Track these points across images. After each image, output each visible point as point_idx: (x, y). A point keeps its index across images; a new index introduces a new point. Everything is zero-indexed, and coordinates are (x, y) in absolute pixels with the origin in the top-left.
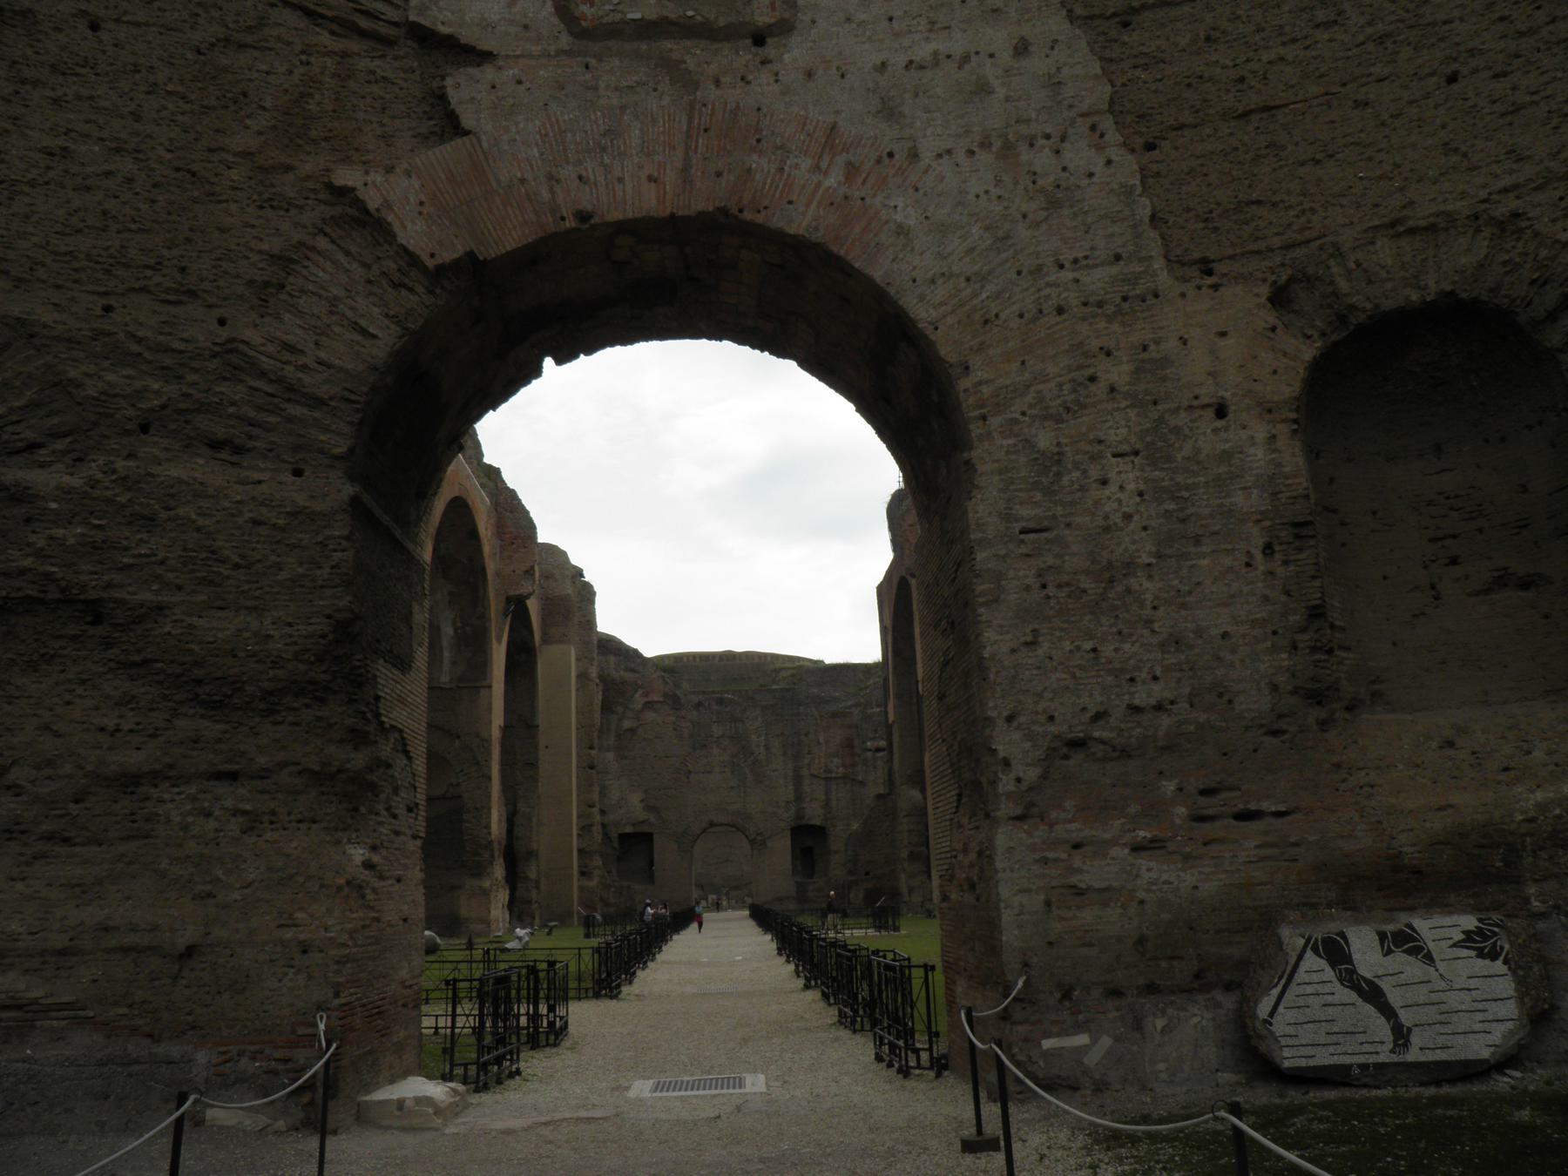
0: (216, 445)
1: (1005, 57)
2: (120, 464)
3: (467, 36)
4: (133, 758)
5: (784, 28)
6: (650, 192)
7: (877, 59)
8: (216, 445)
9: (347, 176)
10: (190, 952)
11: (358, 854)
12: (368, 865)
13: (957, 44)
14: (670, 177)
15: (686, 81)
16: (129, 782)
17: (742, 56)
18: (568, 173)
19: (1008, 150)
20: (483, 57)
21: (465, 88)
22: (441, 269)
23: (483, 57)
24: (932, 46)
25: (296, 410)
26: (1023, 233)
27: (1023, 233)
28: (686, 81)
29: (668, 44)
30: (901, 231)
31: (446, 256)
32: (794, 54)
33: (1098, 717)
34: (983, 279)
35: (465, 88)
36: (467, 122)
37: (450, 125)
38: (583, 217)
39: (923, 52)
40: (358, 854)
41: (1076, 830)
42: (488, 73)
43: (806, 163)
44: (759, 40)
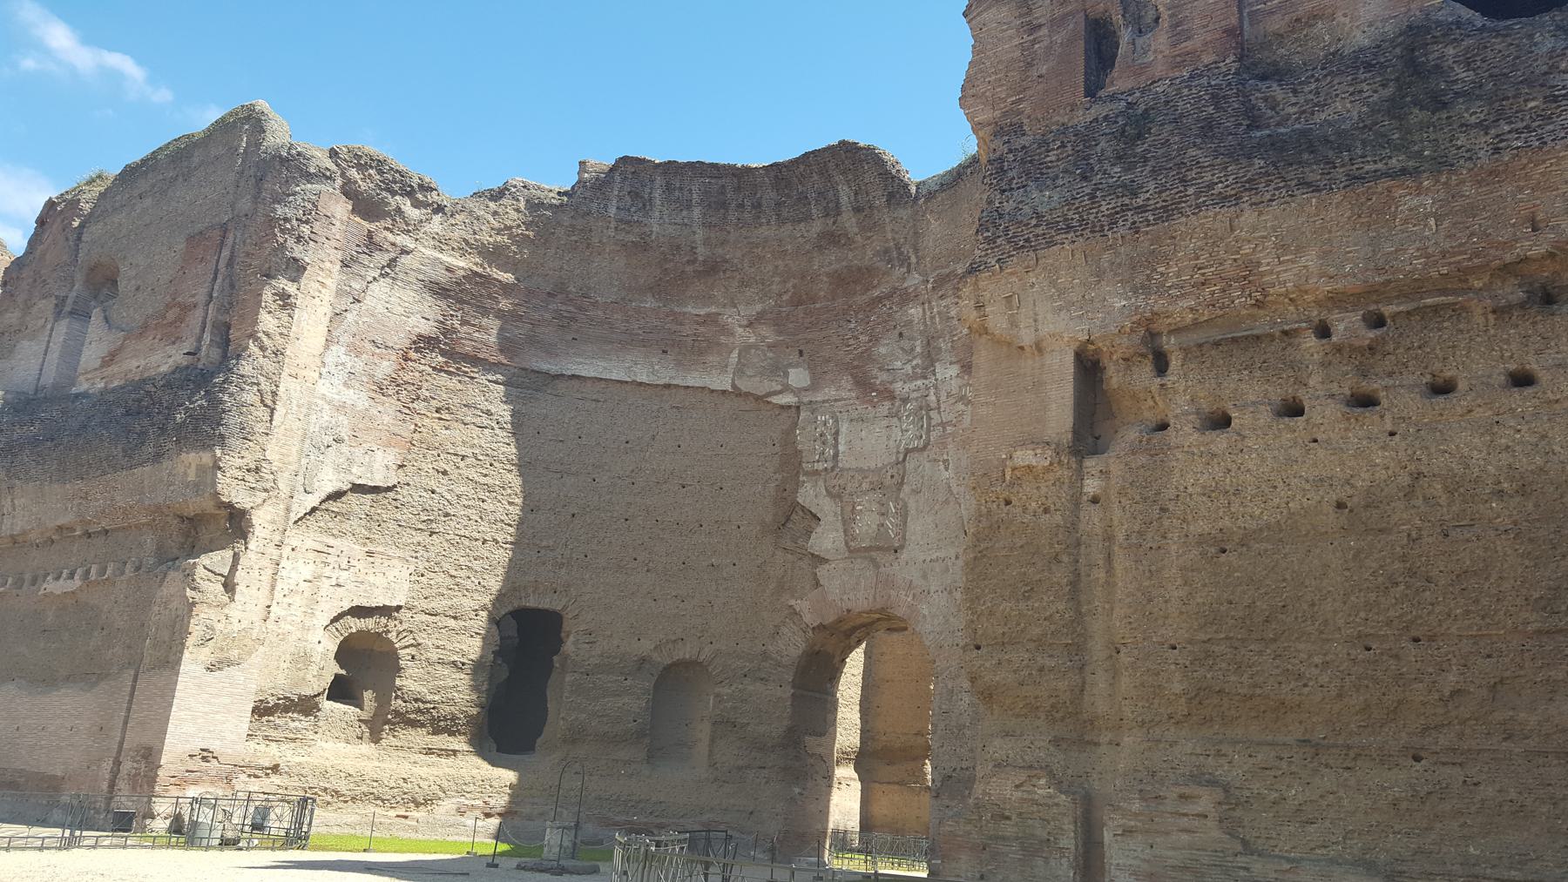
0: (762, 679)
1: (953, 558)
2: (740, 686)
3: (822, 555)
4: (740, 763)
5: (902, 547)
6: (865, 602)
7: (922, 558)
8: (762, 679)
9: (792, 602)
10: (751, 813)
11: (797, 790)
12: (801, 794)
13: (941, 554)
14: (871, 598)
15: (877, 566)
16: (740, 768)
17: (891, 557)
18: (845, 597)
19: (950, 593)
20: (827, 561)
21: (822, 571)
22: (814, 628)
23: (827, 561)
24: (937, 554)
25: (780, 669)
26: (952, 619)
27: (952, 619)
28: (877, 566)
29: (873, 553)
30: (924, 616)
31: (815, 624)
32: (904, 556)
33: (955, 770)
34: (940, 633)
35: (822, 571)
36: (821, 583)
37: (817, 584)
38: (849, 611)
39: (934, 557)
40: (797, 790)
41: (947, 802)
42: (827, 566)
43: (904, 593)
44: (896, 552)
